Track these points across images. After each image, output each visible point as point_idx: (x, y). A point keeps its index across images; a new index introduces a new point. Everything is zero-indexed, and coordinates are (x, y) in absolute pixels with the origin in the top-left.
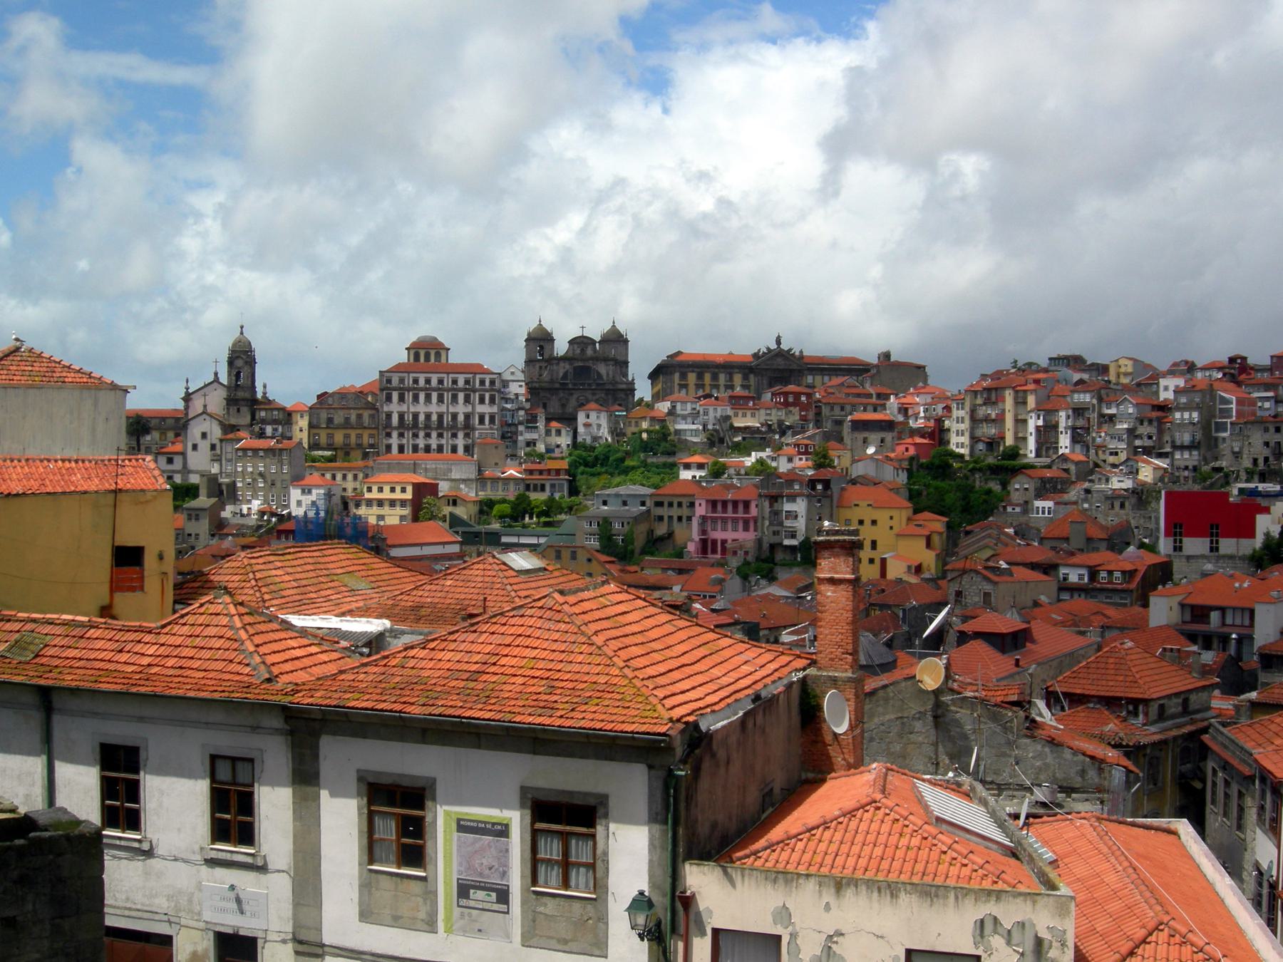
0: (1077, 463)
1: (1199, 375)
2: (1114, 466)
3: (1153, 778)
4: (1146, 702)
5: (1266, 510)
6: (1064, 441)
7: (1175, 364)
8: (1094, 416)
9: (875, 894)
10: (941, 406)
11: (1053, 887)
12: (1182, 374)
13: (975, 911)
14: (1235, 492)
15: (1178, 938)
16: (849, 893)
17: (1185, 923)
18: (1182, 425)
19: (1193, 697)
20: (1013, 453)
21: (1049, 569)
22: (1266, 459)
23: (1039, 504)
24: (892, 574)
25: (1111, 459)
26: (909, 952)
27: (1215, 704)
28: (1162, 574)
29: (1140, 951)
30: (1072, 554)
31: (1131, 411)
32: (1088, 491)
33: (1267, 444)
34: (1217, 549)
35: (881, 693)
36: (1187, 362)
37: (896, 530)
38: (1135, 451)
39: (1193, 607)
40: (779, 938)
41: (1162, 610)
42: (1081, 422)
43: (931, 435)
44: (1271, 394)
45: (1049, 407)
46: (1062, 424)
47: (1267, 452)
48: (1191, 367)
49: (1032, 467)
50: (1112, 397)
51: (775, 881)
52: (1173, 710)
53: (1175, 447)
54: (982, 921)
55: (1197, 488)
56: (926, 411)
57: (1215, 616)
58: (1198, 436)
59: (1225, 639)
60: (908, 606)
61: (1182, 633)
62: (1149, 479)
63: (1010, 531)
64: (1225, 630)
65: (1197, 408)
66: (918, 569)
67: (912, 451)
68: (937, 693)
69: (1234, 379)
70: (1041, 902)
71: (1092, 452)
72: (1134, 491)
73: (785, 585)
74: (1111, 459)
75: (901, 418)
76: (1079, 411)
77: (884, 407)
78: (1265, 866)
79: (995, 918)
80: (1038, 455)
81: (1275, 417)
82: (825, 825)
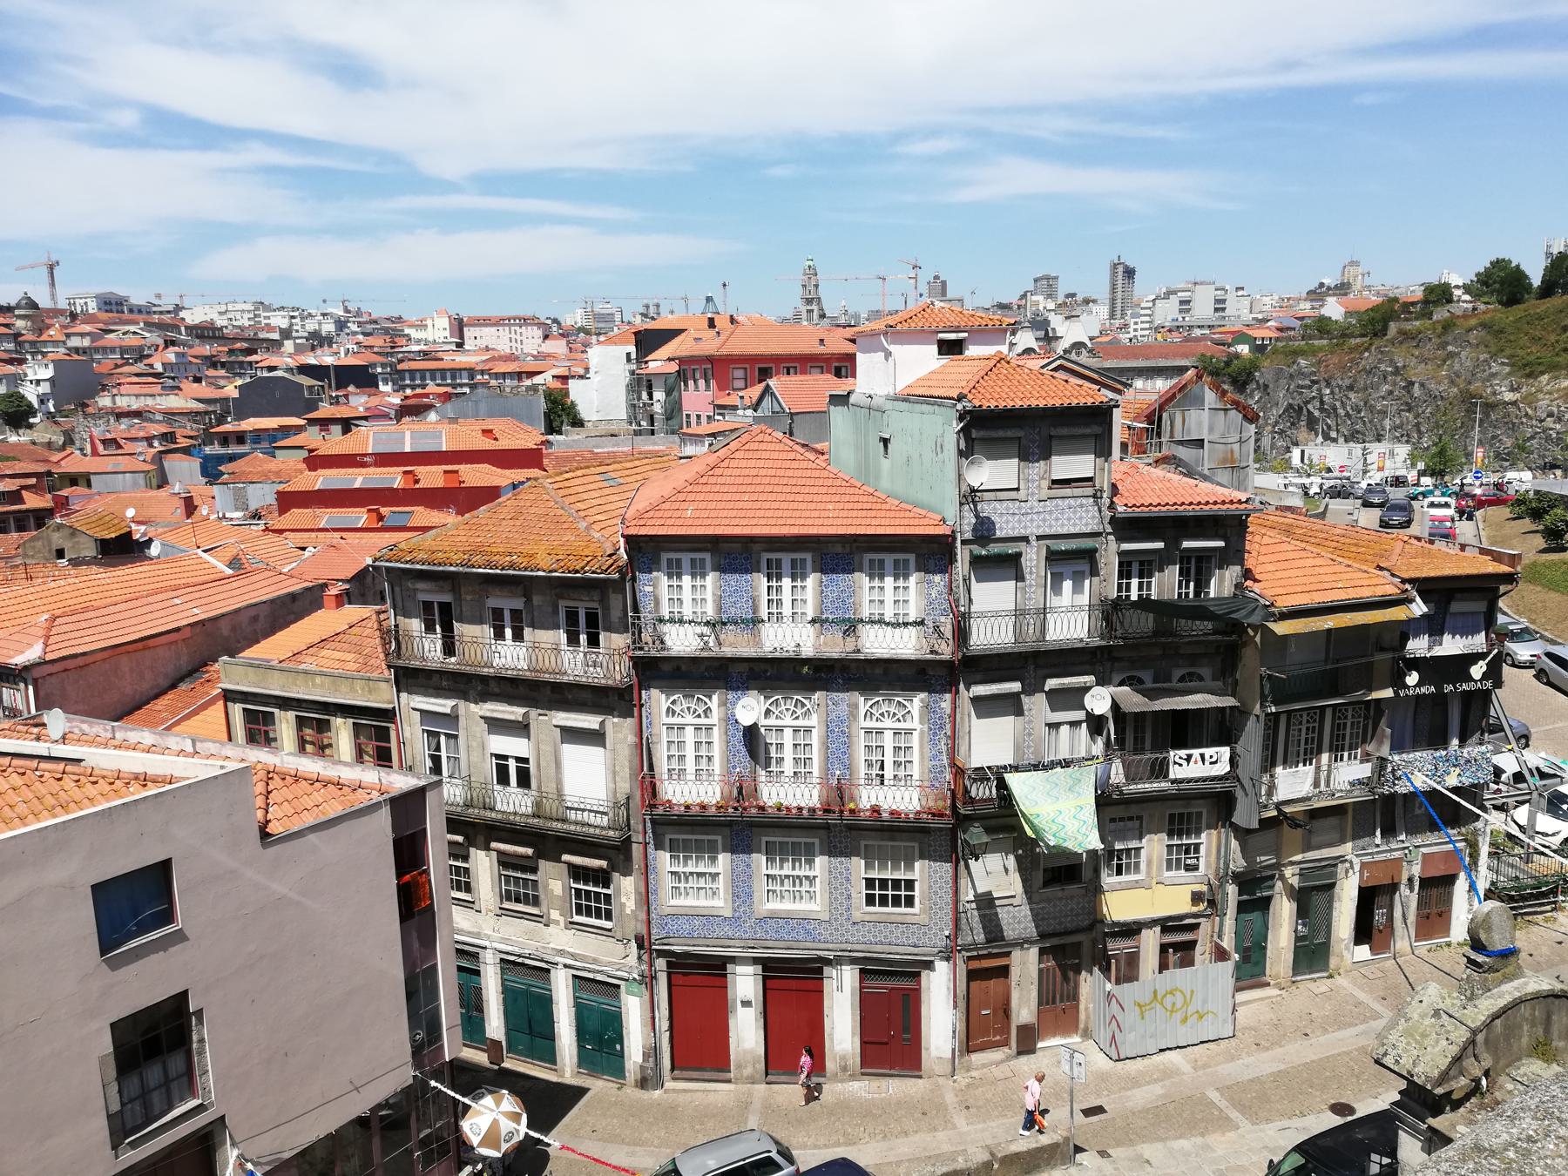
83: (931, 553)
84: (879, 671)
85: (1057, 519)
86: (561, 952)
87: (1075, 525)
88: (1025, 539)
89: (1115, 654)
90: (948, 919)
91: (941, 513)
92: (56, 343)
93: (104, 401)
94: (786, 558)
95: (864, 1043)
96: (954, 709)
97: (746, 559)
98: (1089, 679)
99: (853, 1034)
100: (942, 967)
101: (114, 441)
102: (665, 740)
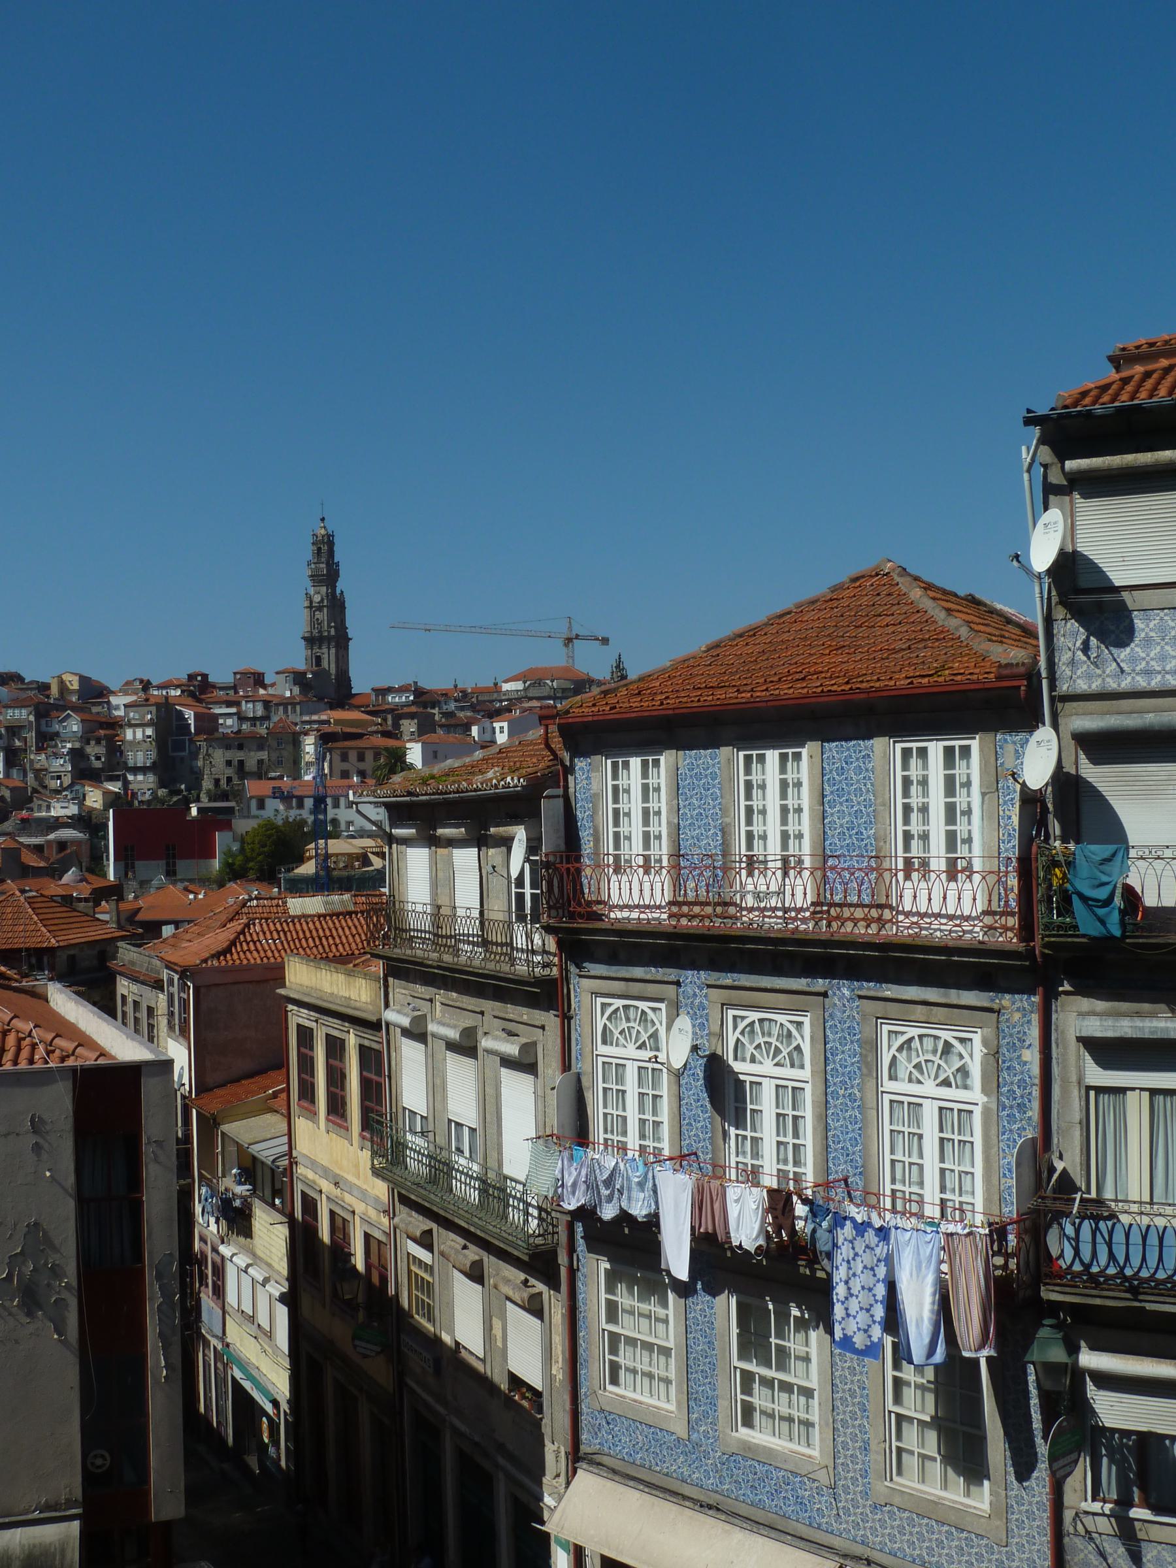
0: (13, 790)
4: (51, 950)
5: (227, 826)
7: (128, 683)
8: (31, 736)
14: (194, 812)
18: (134, 743)
22: (229, 779)
31: (75, 728)
32: (24, 821)
33: (229, 763)
34: (174, 873)
36: (141, 681)
44: (233, 710)
47: (230, 772)
48: (146, 685)
50: (54, 713)
58: (153, 755)
62: (96, 805)
69: (192, 695)
71: (31, 775)
81: (239, 731)
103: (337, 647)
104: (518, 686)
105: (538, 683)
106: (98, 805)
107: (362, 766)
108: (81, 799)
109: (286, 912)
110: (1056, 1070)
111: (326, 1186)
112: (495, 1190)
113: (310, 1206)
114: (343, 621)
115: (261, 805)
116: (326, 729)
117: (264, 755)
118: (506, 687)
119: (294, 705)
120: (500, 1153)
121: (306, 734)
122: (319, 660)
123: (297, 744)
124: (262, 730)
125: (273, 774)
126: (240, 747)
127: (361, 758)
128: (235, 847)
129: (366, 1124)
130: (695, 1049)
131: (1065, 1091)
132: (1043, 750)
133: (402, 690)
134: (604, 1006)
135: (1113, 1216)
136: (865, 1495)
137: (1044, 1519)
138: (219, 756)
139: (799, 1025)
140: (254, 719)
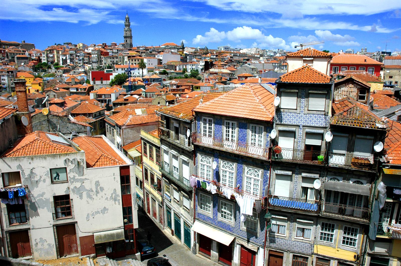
0: (72, 66)
1: (97, 47)
2: (80, 67)
3: (95, 129)
4: (92, 114)
5: (112, 74)
6: (68, 61)
9: (41, 158)
10: (39, 54)
11: (80, 151)
12: (93, 47)
13: (63, 158)
14: (105, 71)
15: (106, 157)
16: (35, 159)
17: (107, 154)
18: (93, 57)
19: (101, 112)
20: (57, 64)
21: (68, 89)
22: (111, 64)
23: (64, 75)
24: (31, 92)
25: (80, 65)
26: (51, 169)
27: (105, 113)
28: (92, 88)
29: (99, 161)
30: (72, 85)
33: (111, 61)
35: (34, 117)
37: (31, 82)
38: (84, 63)
39: (99, 95)
40: (19, 172)
41: (92, 96)
42: (72, 57)
43: (37, 60)
44: (111, 51)
45: (64, 54)
46: (68, 58)
47: (111, 63)
49: (61, 67)
51: (16, 160)
52: (98, 115)
53: (92, 62)
54: (66, 160)
55: (97, 71)
56: (35, 55)
57: (103, 96)
58: (97, 60)
59: (105, 101)
60: (36, 99)
61: (97, 100)
63: (58, 81)
64: (106, 99)
65: (96, 54)
66: (38, 91)
67: (33, 64)
68: (47, 115)
69: (103, 48)
70: (78, 154)
71: (75, 64)
72: (84, 72)
73: (5, 96)
74: (80, 65)
75: (29, 56)
76: (71, 55)
77: (25, 54)
78: (119, 143)
79: (68, 159)
80: (63, 64)
82: (27, 145)
83: (267, 126)
84: (251, 160)
85: (310, 121)
86: (182, 214)
87: (317, 124)
88: (299, 126)
89: (329, 169)
90: (264, 237)
91: (267, 115)
92: (208, 57)
93: (212, 70)
94: (231, 122)
95: (241, 263)
96: (270, 176)
97: (221, 121)
98: (317, 176)
99: (238, 259)
100: (261, 250)
101: (208, 79)
102: (200, 168)
103: (130, 38)
104: (164, 46)
105: (167, 46)
106: (88, 69)
107: (135, 62)
108: (84, 68)
109: (135, 112)
110: (271, 177)
111: (149, 168)
112: (181, 179)
113: (146, 170)
114: (131, 33)
115: (117, 70)
116: (130, 55)
117: (117, 60)
118: (161, 47)
119: (123, 50)
120: (182, 173)
121: (125, 56)
122: (127, 41)
123: (123, 59)
124: (116, 55)
125: (119, 64)
126: (113, 58)
127: (135, 61)
128: (113, 78)
129: (157, 161)
130: (217, 166)
131: (273, 180)
132: (274, 132)
133: (142, 47)
134: (201, 156)
135: (279, 199)
136: (239, 228)
137: (265, 234)
138: (109, 60)
139: (233, 164)
140: (115, 53)
